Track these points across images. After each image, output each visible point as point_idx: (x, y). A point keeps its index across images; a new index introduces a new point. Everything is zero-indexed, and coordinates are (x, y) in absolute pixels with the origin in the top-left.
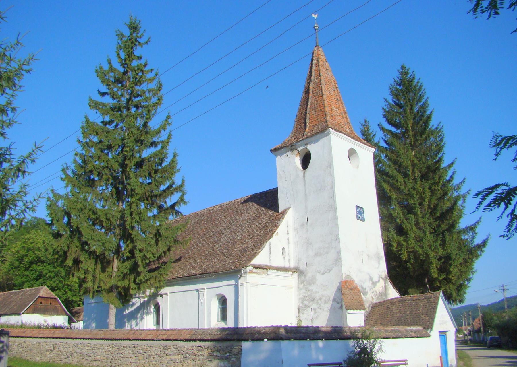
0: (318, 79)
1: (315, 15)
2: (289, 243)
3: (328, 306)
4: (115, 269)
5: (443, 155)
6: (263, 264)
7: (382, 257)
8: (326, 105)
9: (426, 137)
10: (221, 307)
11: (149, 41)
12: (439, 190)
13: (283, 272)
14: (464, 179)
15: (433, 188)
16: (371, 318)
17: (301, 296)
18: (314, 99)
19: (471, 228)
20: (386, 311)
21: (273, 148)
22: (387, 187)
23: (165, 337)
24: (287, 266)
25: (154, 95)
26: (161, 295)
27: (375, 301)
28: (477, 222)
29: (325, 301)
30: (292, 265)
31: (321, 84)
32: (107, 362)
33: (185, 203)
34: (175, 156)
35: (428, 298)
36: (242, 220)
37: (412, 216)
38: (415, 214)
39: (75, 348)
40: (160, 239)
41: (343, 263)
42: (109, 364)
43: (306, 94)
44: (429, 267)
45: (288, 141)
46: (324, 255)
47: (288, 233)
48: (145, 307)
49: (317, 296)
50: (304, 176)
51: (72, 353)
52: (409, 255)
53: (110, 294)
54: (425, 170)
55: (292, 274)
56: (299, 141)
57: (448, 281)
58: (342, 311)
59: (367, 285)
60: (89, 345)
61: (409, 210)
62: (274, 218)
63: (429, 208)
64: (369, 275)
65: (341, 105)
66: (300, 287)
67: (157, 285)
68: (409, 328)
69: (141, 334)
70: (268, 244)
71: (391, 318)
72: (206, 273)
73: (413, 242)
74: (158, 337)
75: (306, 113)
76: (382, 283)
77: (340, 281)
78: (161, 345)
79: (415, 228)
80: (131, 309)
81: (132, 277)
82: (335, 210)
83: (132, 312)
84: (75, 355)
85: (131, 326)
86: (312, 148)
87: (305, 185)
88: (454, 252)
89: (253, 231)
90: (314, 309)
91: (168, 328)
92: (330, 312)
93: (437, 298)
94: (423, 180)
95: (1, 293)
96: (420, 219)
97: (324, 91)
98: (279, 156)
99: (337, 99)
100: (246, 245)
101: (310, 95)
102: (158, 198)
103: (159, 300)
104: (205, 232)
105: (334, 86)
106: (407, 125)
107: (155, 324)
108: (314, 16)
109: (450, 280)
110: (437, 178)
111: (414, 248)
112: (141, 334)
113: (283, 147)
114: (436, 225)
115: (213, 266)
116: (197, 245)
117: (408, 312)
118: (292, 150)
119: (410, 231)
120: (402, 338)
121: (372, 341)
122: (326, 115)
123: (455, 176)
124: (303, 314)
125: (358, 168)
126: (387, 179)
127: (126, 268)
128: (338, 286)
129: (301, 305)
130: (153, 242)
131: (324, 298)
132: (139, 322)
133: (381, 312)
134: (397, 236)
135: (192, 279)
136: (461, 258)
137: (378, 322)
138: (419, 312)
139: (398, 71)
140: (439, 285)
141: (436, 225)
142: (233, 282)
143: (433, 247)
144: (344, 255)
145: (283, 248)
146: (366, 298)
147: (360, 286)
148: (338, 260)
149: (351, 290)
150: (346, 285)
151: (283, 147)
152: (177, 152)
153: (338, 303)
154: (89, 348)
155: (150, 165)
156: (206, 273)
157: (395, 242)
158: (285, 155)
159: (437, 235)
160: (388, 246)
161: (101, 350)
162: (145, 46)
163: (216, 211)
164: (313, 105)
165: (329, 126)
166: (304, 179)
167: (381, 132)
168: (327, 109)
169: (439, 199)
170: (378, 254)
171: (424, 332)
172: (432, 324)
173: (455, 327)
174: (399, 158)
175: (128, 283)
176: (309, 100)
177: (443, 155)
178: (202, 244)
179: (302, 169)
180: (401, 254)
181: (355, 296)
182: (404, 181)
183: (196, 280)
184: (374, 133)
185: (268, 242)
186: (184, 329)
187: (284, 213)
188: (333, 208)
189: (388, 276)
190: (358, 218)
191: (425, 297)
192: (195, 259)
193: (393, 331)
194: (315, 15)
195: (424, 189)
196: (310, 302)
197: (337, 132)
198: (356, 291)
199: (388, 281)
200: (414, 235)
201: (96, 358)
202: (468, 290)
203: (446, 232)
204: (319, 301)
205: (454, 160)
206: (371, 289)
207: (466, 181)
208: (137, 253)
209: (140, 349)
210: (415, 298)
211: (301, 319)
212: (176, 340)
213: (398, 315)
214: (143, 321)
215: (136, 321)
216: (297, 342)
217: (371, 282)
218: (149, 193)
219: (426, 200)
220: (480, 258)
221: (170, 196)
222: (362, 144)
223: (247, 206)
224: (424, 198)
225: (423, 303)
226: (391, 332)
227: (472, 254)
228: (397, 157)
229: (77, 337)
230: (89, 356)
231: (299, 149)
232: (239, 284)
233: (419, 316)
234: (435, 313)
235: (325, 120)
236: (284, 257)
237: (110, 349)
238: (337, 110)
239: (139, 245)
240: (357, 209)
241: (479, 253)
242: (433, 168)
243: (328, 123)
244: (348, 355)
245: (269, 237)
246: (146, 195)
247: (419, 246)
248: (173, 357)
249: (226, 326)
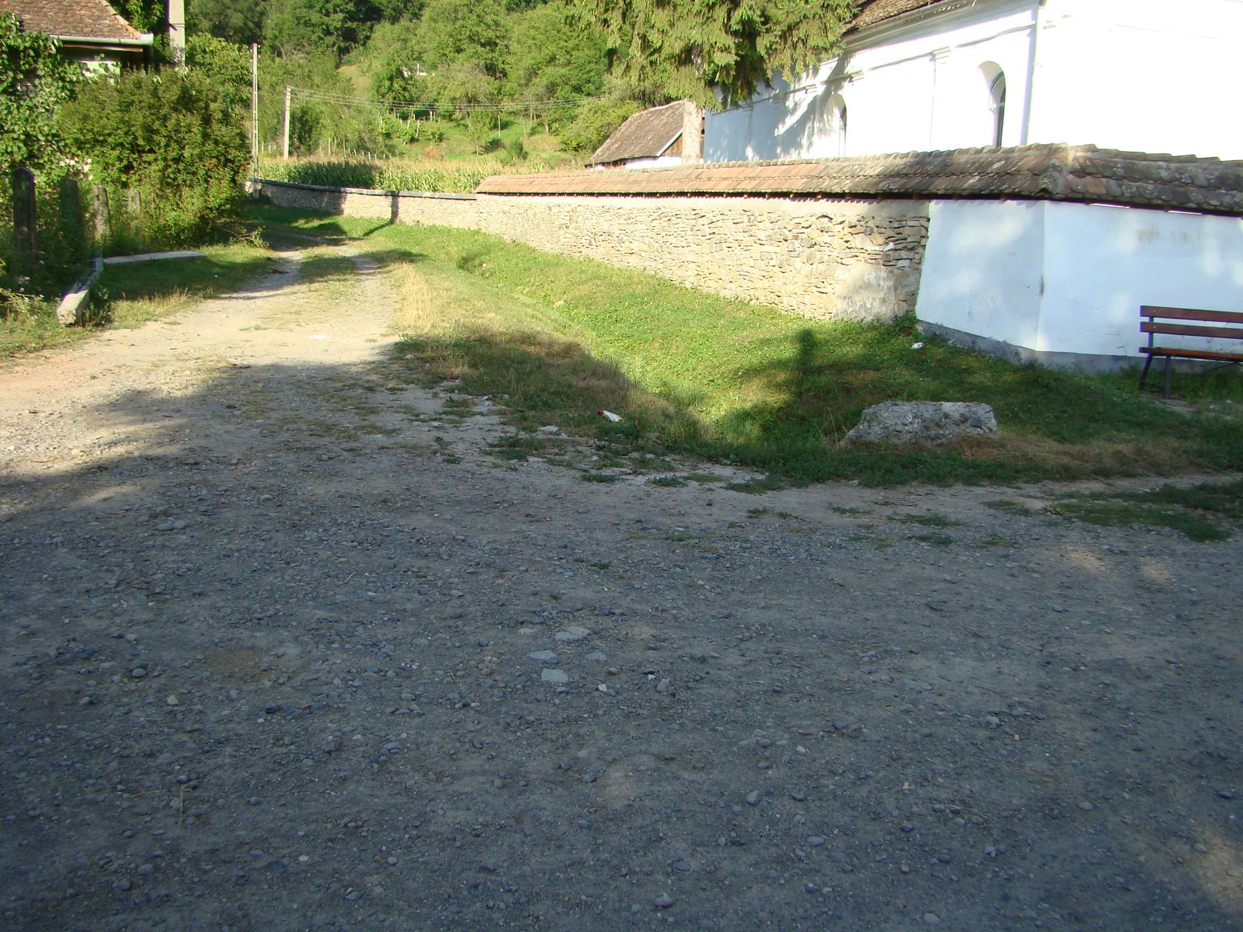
48: (817, 116)
95: (105, 3)
135: (920, 19)
212: (774, 195)
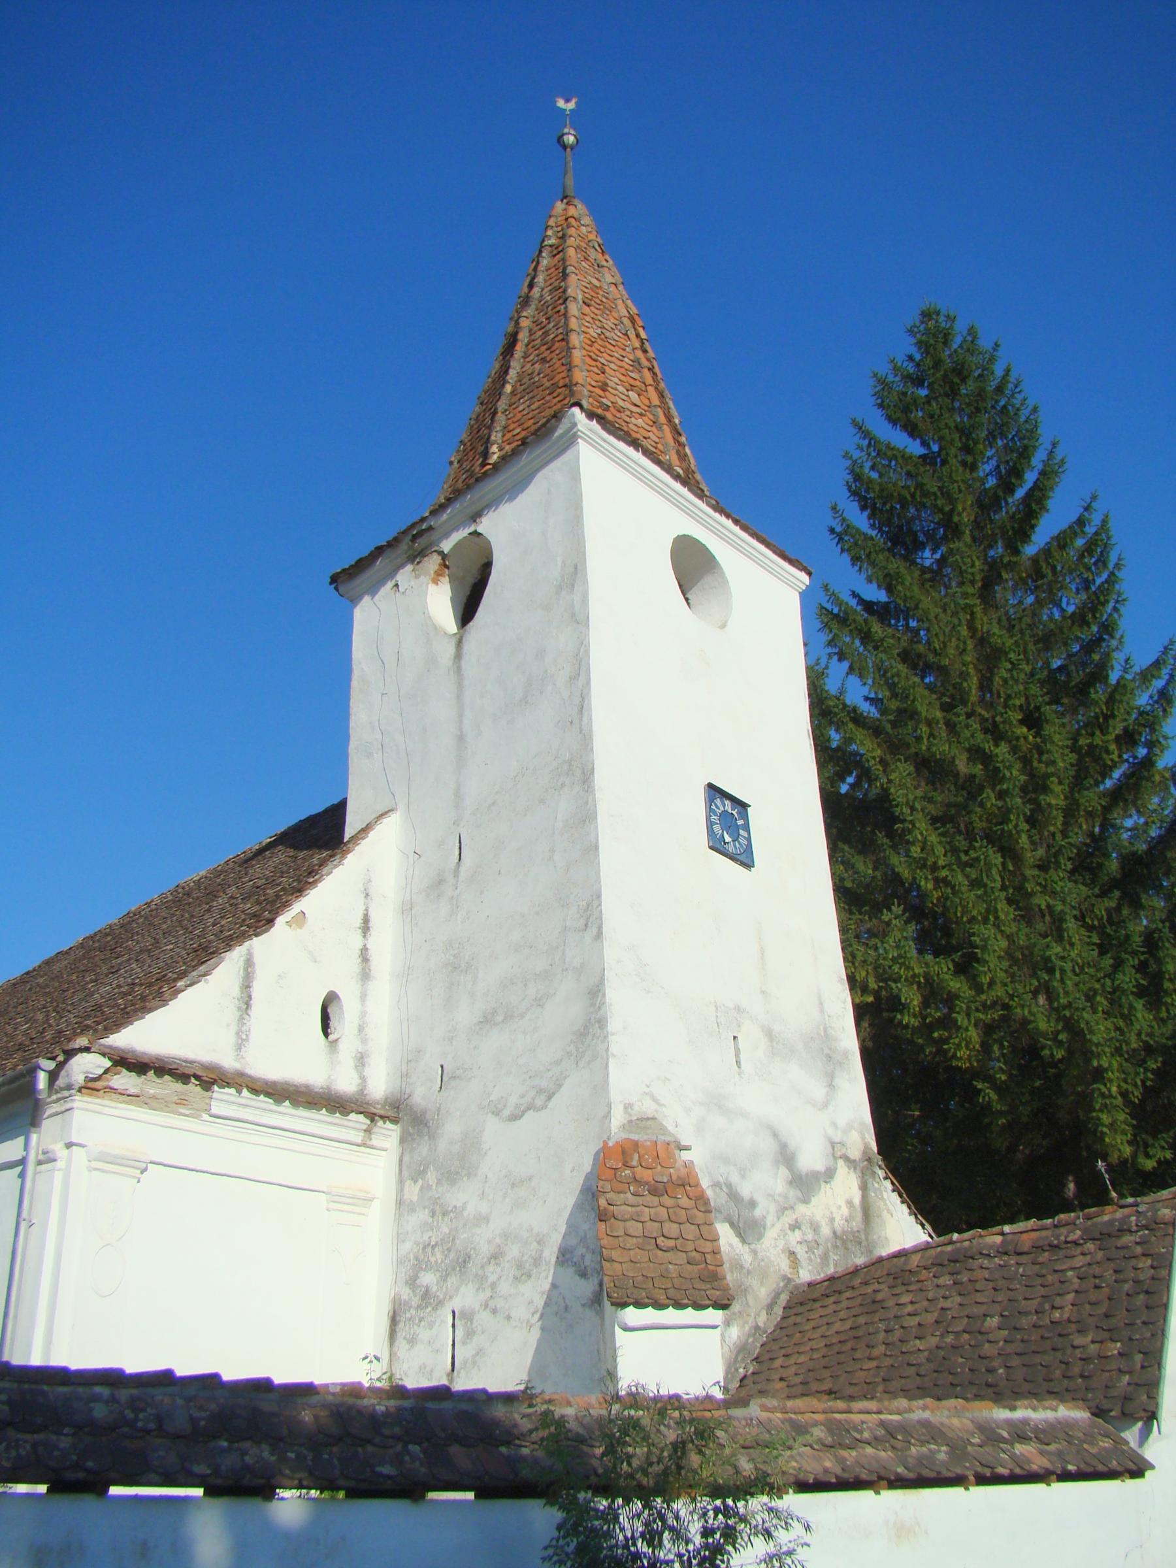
1: (567, 101)
2: (365, 975)
5: (1115, 609)
6: (191, 1056)
7: (846, 1054)
16: (778, 1363)
17: (408, 1246)
20: (861, 1320)
24: (346, 1083)
27: (806, 1275)
29: (520, 1266)
30: (379, 1087)
35: (1103, 1237)
46: (522, 1016)
47: (366, 927)
49: (483, 1239)
55: (368, 1131)
58: (602, 1318)
64: (775, 1135)
66: (407, 1196)
68: (1002, 1414)
71: (888, 1362)
77: (595, 1146)
79: (1005, 911)
82: (586, 778)
87: (459, 697)
92: (543, 1329)
98: (367, 599)
108: (561, 103)
118: (416, 557)
120: (957, 1481)
124: (412, 1341)
125: (723, 626)
128: (588, 1177)
129: (406, 1293)
131: (513, 1251)
133: (838, 1326)
134: (921, 952)
137: (815, 1386)
138: (1057, 1315)
139: (911, 332)
146: (754, 1252)
147: (716, 1185)
149: (654, 1192)
150: (626, 1165)
153: (583, 1274)
157: (912, 980)
158: (390, 584)
172: (1150, 1384)
177: (1115, 609)
181: (672, 1229)
191: (1085, 1231)
194: (567, 101)
196: (444, 1278)
197: (611, 439)
198: (684, 1201)
199: (881, 1173)
200: (1004, 944)
204: (491, 1268)
206: (783, 1210)
210: (1027, 1241)
213: (934, 1341)
217: (784, 1172)
225: (1079, 1261)
231: (447, 546)
233: (1059, 1342)
234: (1165, 1318)
238: (633, 395)
240: (710, 801)
242: (1078, 676)
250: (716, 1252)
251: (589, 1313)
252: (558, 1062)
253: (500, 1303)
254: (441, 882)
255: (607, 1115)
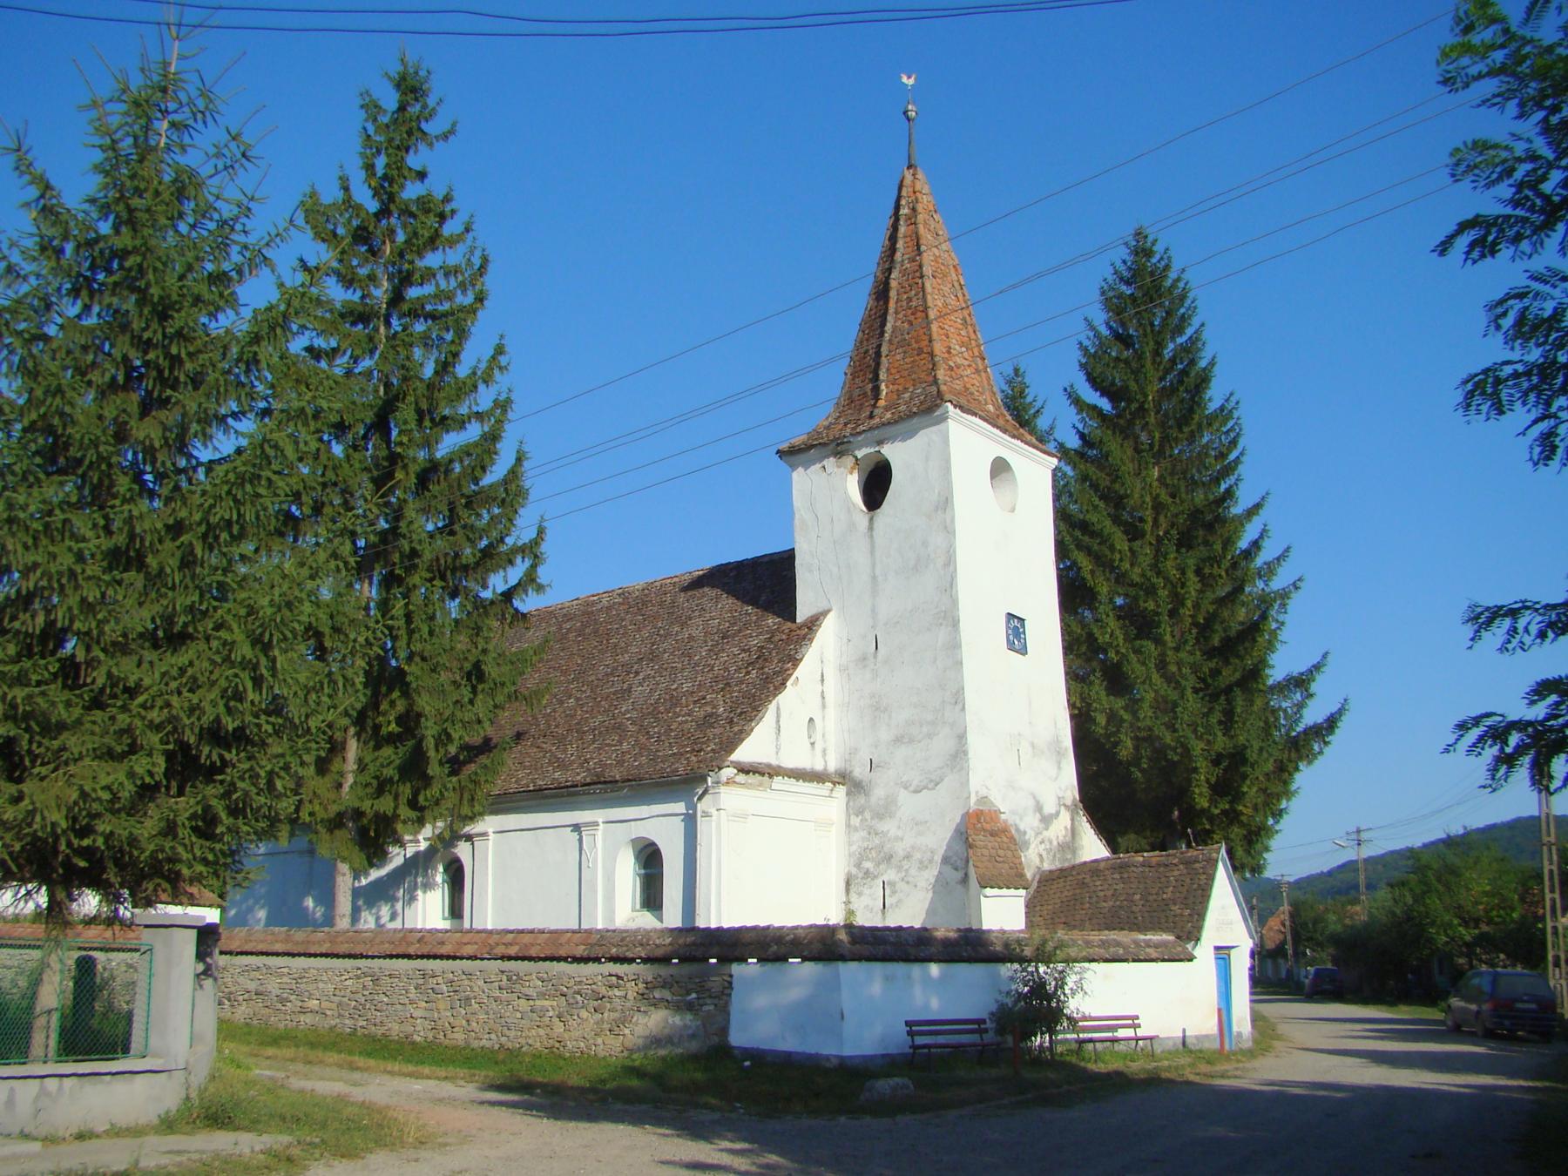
0: (912, 260)
2: (824, 706)
3: (931, 874)
4: (351, 765)
8: (935, 336)
9: (1192, 431)
10: (643, 871)
11: (452, 132)
12: (1220, 575)
13: (811, 785)
14: (1287, 550)
15: (1207, 571)
16: (1038, 908)
17: (854, 848)
18: (900, 316)
19: (1300, 683)
21: (784, 446)
22: (1085, 563)
23: (513, 951)
24: (819, 767)
25: (463, 286)
26: (469, 838)
27: (1047, 866)
28: (1317, 667)
29: (921, 862)
30: (832, 767)
31: (922, 277)
32: (340, 1015)
33: (540, 588)
34: (519, 460)
35: (1188, 863)
36: (691, 638)
37: (1149, 646)
38: (1158, 641)
39: (241, 979)
40: (480, 687)
41: (972, 763)
42: (347, 1022)
43: (877, 299)
44: (1189, 781)
45: (828, 428)
47: (822, 680)
49: (900, 849)
50: (871, 528)
51: (231, 993)
52: (1137, 748)
53: (337, 832)
54: (1185, 520)
56: (860, 433)
57: (1232, 817)
58: (967, 888)
59: (1027, 823)
60: (285, 970)
61: (1140, 624)
62: (784, 637)
63: (1195, 624)
64: (1034, 797)
65: (973, 336)
67: (466, 810)
68: (1142, 937)
69: (443, 943)
70: (772, 707)
72: (605, 782)
73: (1150, 714)
74: (495, 951)
75: (878, 354)
76: (1065, 819)
77: (961, 812)
78: (503, 972)
79: (1156, 677)
80: (375, 874)
81: (406, 790)
82: (955, 624)
83: (378, 882)
84: (241, 998)
85: (378, 919)
86: (896, 453)
88: (1256, 745)
89: (726, 669)
90: (889, 883)
91: (490, 927)
93: (1213, 863)
94: (1183, 550)
96: (1170, 653)
97: (929, 297)
98: (800, 469)
99: (964, 319)
100: (709, 709)
101: (892, 305)
102: (471, 572)
103: (463, 850)
104: (581, 665)
105: (956, 284)
106: (1146, 396)
107: (446, 914)
109: (1238, 814)
110: (1218, 547)
111: (1150, 729)
112: (443, 943)
113: (813, 446)
114: (1211, 670)
115: (620, 763)
116: (561, 702)
117: (1137, 897)
119: (1144, 683)
121: (1060, 966)
122: (934, 365)
123: (1265, 543)
124: (860, 894)
125: (1013, 510)
126: (1086, 538)
127: (389, 765)
128: (958, 825)
129: (854, 871)
130: (466, 692)
131: (918, 856)
132: (400, 911)
133: (1066, 893)
134: (1108, 695)
136: (1272, 760)
140: (1208, 827)
141: (1211, 670)
142: (680, 807)
143: (1200, 729)
144: (976, 744)
145: (811, 720)
148: (959, 755)
149: (992, 835)
151: (813, 446)
152: (526, 448)
153: (956, 869)
154: (285, 979)
155: (455, 484)
156: (605, 782)
158: (818, 466)
159: (1210, 695)
160: (1081, 720)
161: (321, 985)
162: (439, 145)
163: (609, 608)
164: (898, 334)
165: (947, 397)
166: (871, 537)
167: (1073, 410)
168: (938, 348)
169: (1221, 602)
170: (1058, 741)
171: (1180, 949)
173: (1252, 937)
174: (1117, 486)
175: (392, 805)
176: (889, 318)
178: (578, 699)
179: (864, 509)
180: (1116, 744)
181: (1001, 852)
182: (1131, 549)
183: (574, 799)
184: (1038, 405)
185: (774, 702)
186: (567, 931)
187: (813, 624)
188: (950, 619)
189: (1081, 801)
190: (1011, 647)
192: (562, 742)
193: (1103, 944)
195: (1183, 573)
197: (965, 415)
198: (1005, 839)
200: (1153, 695)
201: (305, 1005)
202: (1274, 843)
203: (1237, 691)
204: (905, 862)
205: (1263, 498)
206: (1038, 834)
207: (1292, 554)
208: (426, 728)
209: (440, 981)
210: (1154, 861)
211: (851, 907)
213: (1111, 903)
214: (413, 905)
215: (393, 906)
216: (878, 968)
217: (1038, 815)
218: (449, 560)
219: (1189, 603)
220: (1319, 762)
221: (505, 569)
222: (1026, 447)
223: (699, 599)
224: (1184, 599)
225: (1176, 873)
226: (1099, 946)
227: (1298, 750)
228: (1113, 482)
229: (247, 948)
230: (283, 1001)
231: (860, 454)
232: (699, 814)
235: (931, 379)
236: (813, 744)
237: (347, 983)
239: (424, 703)
240: (1008, 622)
241: (1316, 747)
243: (943, 388)
244: (997, 1001)
245: (776, 688)
246: (439, 565)
247: (1164, 724)
248: (538, 1003)
249: (657, 925)
250: (1021, 863)
251: (959, 887)
252: (942, 768)
253: (910, 879)
254: (864, 659)
255: (969, 797)
